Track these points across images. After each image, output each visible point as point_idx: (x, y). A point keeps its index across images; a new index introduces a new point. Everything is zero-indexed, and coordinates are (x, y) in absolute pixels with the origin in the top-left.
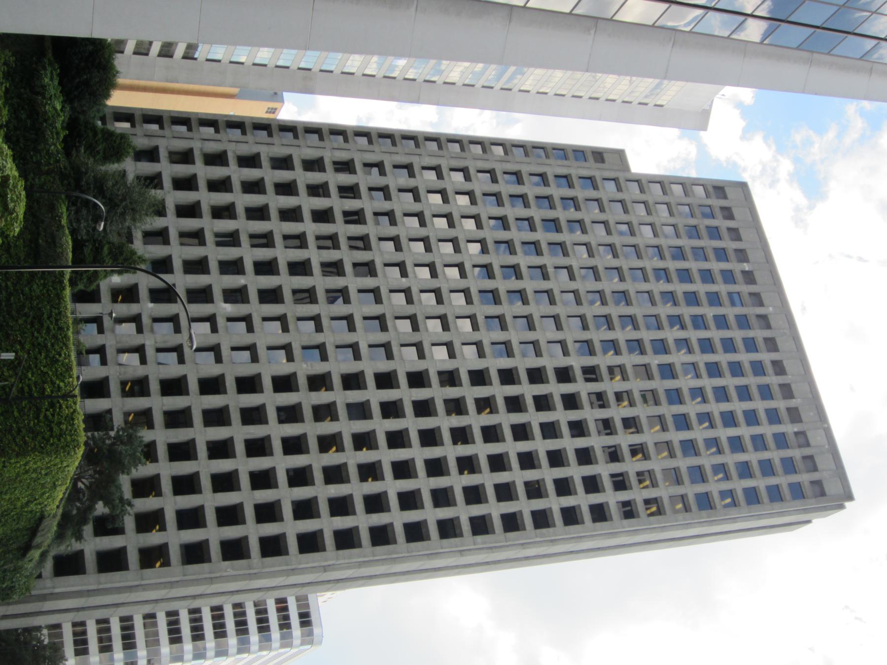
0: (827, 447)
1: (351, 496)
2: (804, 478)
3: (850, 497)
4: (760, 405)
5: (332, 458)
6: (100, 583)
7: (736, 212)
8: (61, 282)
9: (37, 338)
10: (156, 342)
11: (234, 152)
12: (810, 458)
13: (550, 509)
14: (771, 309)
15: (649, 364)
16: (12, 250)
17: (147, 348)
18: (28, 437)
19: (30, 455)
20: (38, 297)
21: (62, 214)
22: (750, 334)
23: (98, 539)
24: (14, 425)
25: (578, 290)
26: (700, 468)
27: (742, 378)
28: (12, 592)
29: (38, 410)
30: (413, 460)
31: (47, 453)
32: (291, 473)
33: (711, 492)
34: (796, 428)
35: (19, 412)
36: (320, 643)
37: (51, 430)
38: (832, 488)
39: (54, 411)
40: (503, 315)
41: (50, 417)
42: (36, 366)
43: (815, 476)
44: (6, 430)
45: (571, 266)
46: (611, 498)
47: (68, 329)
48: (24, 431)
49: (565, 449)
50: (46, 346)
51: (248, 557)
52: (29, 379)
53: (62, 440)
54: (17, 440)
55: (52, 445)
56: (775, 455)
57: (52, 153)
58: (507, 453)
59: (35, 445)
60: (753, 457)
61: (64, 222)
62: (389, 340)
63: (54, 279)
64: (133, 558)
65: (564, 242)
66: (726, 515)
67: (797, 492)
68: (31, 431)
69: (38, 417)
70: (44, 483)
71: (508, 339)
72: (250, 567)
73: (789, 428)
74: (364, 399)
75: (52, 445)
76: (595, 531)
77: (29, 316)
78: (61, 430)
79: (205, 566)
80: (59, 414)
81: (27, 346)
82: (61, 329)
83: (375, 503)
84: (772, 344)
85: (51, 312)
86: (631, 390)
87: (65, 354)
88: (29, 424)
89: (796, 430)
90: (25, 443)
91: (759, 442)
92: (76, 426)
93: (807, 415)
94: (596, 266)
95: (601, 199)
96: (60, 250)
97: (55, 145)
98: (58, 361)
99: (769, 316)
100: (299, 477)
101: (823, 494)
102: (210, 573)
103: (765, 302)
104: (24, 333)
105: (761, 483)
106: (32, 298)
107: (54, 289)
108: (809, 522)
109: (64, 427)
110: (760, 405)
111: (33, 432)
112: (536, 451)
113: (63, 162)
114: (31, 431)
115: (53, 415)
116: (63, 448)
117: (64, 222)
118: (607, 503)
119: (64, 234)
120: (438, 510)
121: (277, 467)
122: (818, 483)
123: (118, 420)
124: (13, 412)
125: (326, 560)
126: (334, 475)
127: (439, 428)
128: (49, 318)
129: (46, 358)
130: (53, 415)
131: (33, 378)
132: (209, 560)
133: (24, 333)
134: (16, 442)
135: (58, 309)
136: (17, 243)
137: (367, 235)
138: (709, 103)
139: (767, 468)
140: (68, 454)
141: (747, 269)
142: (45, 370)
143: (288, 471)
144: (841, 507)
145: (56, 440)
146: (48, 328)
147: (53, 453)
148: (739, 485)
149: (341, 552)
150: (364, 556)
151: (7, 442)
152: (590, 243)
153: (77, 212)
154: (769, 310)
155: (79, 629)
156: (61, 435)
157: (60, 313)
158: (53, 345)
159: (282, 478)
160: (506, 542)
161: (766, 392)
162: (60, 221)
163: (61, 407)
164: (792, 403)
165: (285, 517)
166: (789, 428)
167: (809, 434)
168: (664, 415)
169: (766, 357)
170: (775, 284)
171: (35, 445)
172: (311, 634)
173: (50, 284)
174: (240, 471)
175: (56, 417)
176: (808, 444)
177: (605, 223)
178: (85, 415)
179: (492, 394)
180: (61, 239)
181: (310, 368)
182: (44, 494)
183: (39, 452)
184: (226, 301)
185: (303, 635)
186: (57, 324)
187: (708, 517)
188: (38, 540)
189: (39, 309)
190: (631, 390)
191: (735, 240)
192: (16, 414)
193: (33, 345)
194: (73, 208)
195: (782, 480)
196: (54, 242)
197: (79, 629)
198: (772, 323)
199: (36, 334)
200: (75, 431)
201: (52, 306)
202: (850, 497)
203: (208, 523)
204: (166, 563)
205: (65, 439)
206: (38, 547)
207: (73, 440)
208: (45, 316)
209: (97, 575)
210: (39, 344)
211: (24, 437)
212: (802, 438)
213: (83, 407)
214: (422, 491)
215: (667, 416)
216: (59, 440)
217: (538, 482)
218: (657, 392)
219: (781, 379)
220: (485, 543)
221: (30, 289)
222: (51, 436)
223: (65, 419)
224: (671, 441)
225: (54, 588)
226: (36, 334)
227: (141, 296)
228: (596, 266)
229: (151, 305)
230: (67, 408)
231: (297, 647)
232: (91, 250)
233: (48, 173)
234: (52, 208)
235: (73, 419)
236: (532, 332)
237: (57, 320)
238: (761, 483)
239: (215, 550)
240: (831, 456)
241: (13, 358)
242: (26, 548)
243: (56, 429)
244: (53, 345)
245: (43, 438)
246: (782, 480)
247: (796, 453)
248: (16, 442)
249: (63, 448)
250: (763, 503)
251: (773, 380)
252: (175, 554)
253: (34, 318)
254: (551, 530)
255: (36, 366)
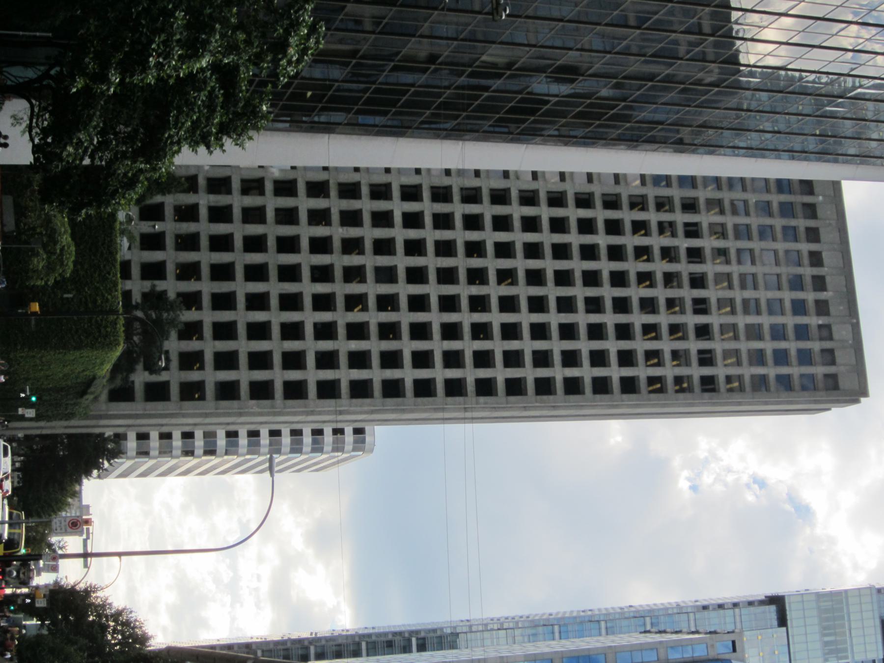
0: (850, 342)
10: (209, 202)
14: (821, 198)
17: (200, 207)
22: (793, 222)
24: (74, 327)
36: (371, 451)
37: (100, 332)
41: (100, 322)
52: (86, 292)
64: (175, 391)
72: (273, 407)
78: (107, 332)
81: (86, 266)
89: (820, 322)
101: (836, 387)
108: (829, 409)
109: (109, 330)
128: (103, 244)
142: (98, 285)
144: (857, 401)
148: (748, 371)
149: (354, 401)
156: (106, 336)
158: (105, 266)
164: (823, 295)
166: (813, 321)
172: (363, 441)
175: (104, 322)
185: (355, 442)
188: (92, 389)
206: (92, 393)
216: (105, 339)
226: (93, 257)
231: (349, 452)
235: (116, 324)
242: (83, 393)
243: (103, 330)
244: (105, 266)
247: (816, 346)
252: (210, 390)
254: (551, 397)
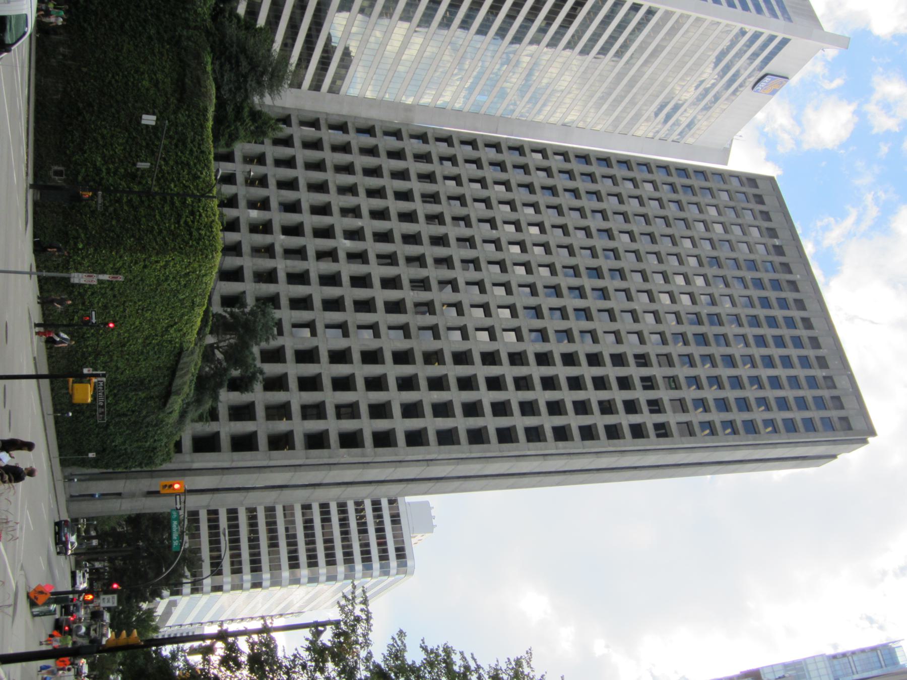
0: (851, 390)
1: (451, 401)
2: (834, 414)
3: (873, 433)
4: (794, 353)
5: (435, 370)
6: (233, 461)
7: (766, 199)
8: (205, 116)
9: (181, 157)
10: (286, 267)
11: (353, 124)
12: (837, 399)
13: (620, 424)
14: (798, 276)
15: (699, 313)
16: (160, 85)
17: (278, 271)
18: (169, 238)
19: (170, 254)
20: (183, 125)
21: (207, 62)
22: (783, 295)
23: (233, 423)
24: (156, 227)
25: (638, 250)
26: (745, 399)
27: (777, 330)
28: (155, 454)
29: (179, 216)
30: (504, 375)
31: (186, 254)
32: (400, 382)
33: (755, 420)
34: (824, 373)
35: (161, 216)
36: (412, 573)
37: (191, 234)
38: (856, 423)
39: (194, 218)
40: (577, 265)
41: (190, 223)
42: (179, 180)
43: (842, 413)
44: (147, 231)
45: (632, 231)
46: (671, 418)
47: (210, 153)
48: (165, 232)
49: (631, 376)
50: (188, 164)
51: (363, 446)
52: (171, 190)
53: (201, 243)
54: (158, 240)
55: (191, 247)
56: (808, 394)
57: (200, 14)
58: (583, 376)
59: (175, 245)
60: (789, 394)
61: (209, 68)
62: (482, 278)
63: (198, 112)
64: (262, 441)
65: (626, 212)
66: (769, 439)
67: (828, 424)
68: (171, 233)
69: (178, 222)
70: (184, 299)
71: (581, 284)
72: (363, 455)
73: (819, 373)
74: (462, 325)
75: (191, 247)
76: (659, 444)
77: (174, 139)
78: (200, 234)
79: (325, 452)
80: (198, 222)
81: (171, 163)
82: (203, 152)
83: (472, 409)
84: (800, 304)
85: (195, 137)
86: (685, 333)
87: (206, 173)
88: (170, 227)
89: (824, 374)
90: (166, 243)
91: (794, 382)
92: (214, 234)
93: (833, 363)
94: (653, 233)
95: (655, 181)
96: (203, 90)
97: (202, 8)
98: (199, 178)
99: (797, 283)
100: (406, 384)
101: (850, 428)
102: (330, 457)
103: (793, 270)
104: (168, 152)
105: (798, 416)
106: (177, 126)
107: (198, 120)
108: (834, 457)
109: (203, 232)
110: (794, 353)
111: (173, 235)
112: (607, 376)
113: (209, 23)
114: (171, 233)
115: (193, 222)
116: (201, 250)
117: (209, 68)
118: (668, 422)
119: (208, 78)
120: (525, 418)
121: (388, 374)
122: (844, 420)
123: (250, 301)
124: (155, 216)
125: (429, 453)
126: (437, 384)
127: (525, 352)
128: (192, 142)
129: (188, 174)
130: (193, 222)
131: (176, 189)
132: (329, 447)
133: (168, 152)
134: (156, 242)
135: (202, 136)
136: (165, 80)
137: (464, 195)
138: (729, 143)
139: (802, 403)
140: (206, 257)
141: (777, 244)
142: (187, 184)
143: (397, 379)
144: (864, 442)
145: (194, 243)
146: (191, 151)
147: (192, 255)
148: (779, 416)
149: (442, 447)
150: (463, 453)
151: (148, 240)
152: (647, 214)
153: (221, 66)
154: (797, 277)
155: (213, 516)
156: (200, 239)
157: (203, 140)
158: (195, 164)
159: (392, 383)
160: (584, 448)
161: (798, 342)
162: (205, 68)
163: (200, 215)
164: (820, 352)
165: (394, 415)
166: (819, 373)
167: (836, 379)
168: (713, 354)
169: (796, 314)
170: (801, 257)
171: (175, 245)
172: (405, 565)
173: (194, 115)
174: (356, 375)
175: (196, 223)
176: (835, 387)
177: (659, 200)
178: (224, 243)
179: (569, 327)
180: (205, 81)
181: (416, 295)
182: (183, 315)
183: (179, 252)
184: (346, 239)
185: (399, 566)
186: (199, 148)
187: (754, 440)
188: (177, 382)
189: (184, 134)
190: (685, 333)
191: (766, 220)
192: (157, 217)
193: (177, 163)
194: (218, 62)
195: (816, 415)
196: (199, 82)
197: (213, 516)
198: (800, 288)
199: (179, 154)
200: (214, 237)
201: (195, 133)
202: (873, 433)
203: (328, 416)
204: (292, 447)
205: (204, 243)
206: (178, 393)
207: (212, 245)
208: (189, 140)
209: (231, 453)
210: (182, 162)
211: (164, 238)
212: (830, 382)
213: (224, 238)
214: (511, 401)
215: (716, 356)
216: (198, 243)
217: (609, 401)
218: (707, 336)
219: (810, 333)
220: (565, 448)
221: (176, 118)
222: (191, 239)
223: (204, 227)
224: (720, 376)
225: (192, 462)
226: (179, 154)
227: (274, 229)
228: (653, 233)
229: (283, 237)
230: (207, 217)
231: (394, 575)
232: (233, 110)
233: (196, 28)
234: (198, 57)
235: (212, 227)
236: (601, 280)
237: (199, 145)
238: (798, 416)
239: (334, 439)
240: (855, 398)
241: (153, 123)
242: (167, 395)
243: (195, 233)
244: (195, 164)
245: (183, 240)
246: (816, 415)
247: (826, 393)
248: (156, 242)
249: (201, 250)
250: (799, 432)
251: (803, 333)
252: (299, 440)
253: (178, 140)
254: (621, 441)
255: (179, 180)
